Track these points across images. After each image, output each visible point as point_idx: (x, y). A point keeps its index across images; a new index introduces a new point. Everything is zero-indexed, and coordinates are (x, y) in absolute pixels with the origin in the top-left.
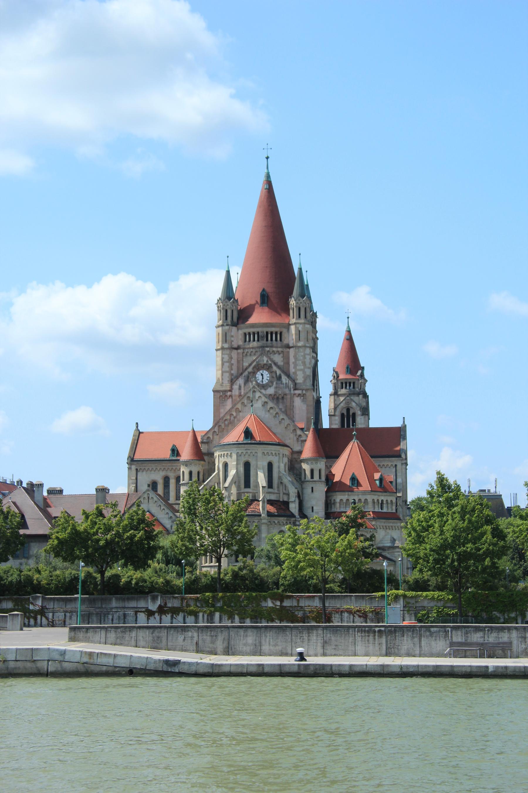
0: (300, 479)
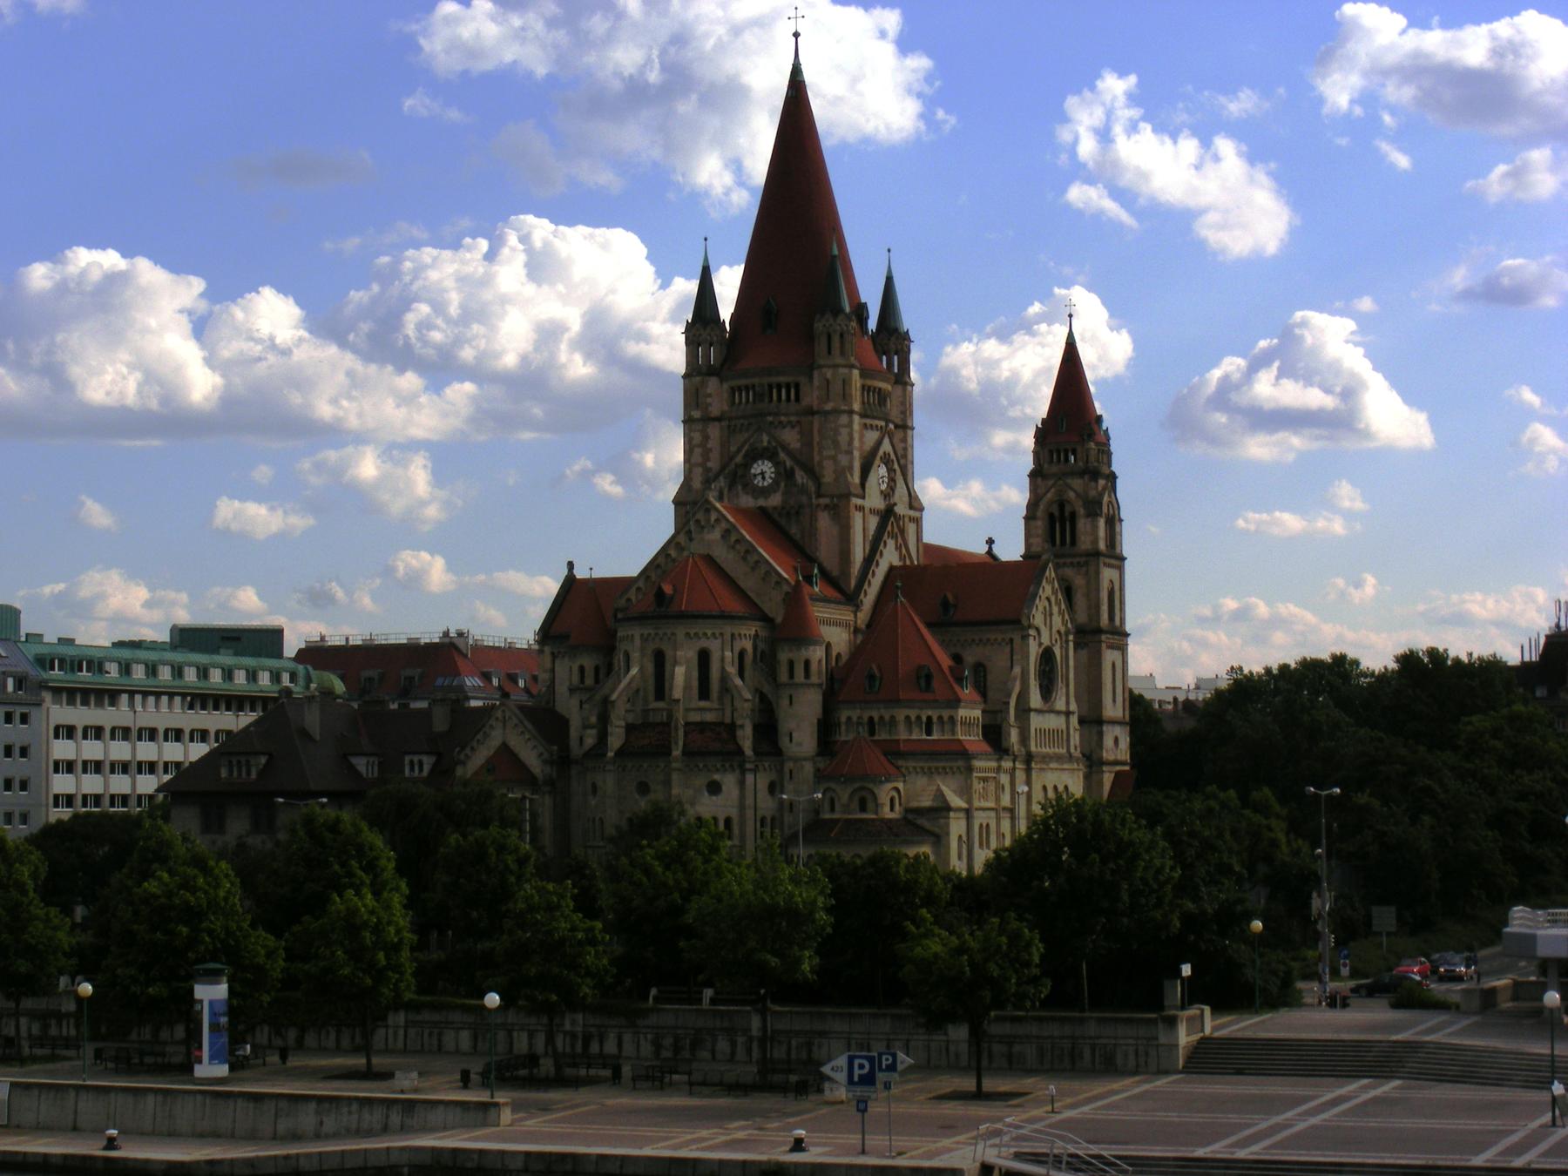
0: (775, 679)
